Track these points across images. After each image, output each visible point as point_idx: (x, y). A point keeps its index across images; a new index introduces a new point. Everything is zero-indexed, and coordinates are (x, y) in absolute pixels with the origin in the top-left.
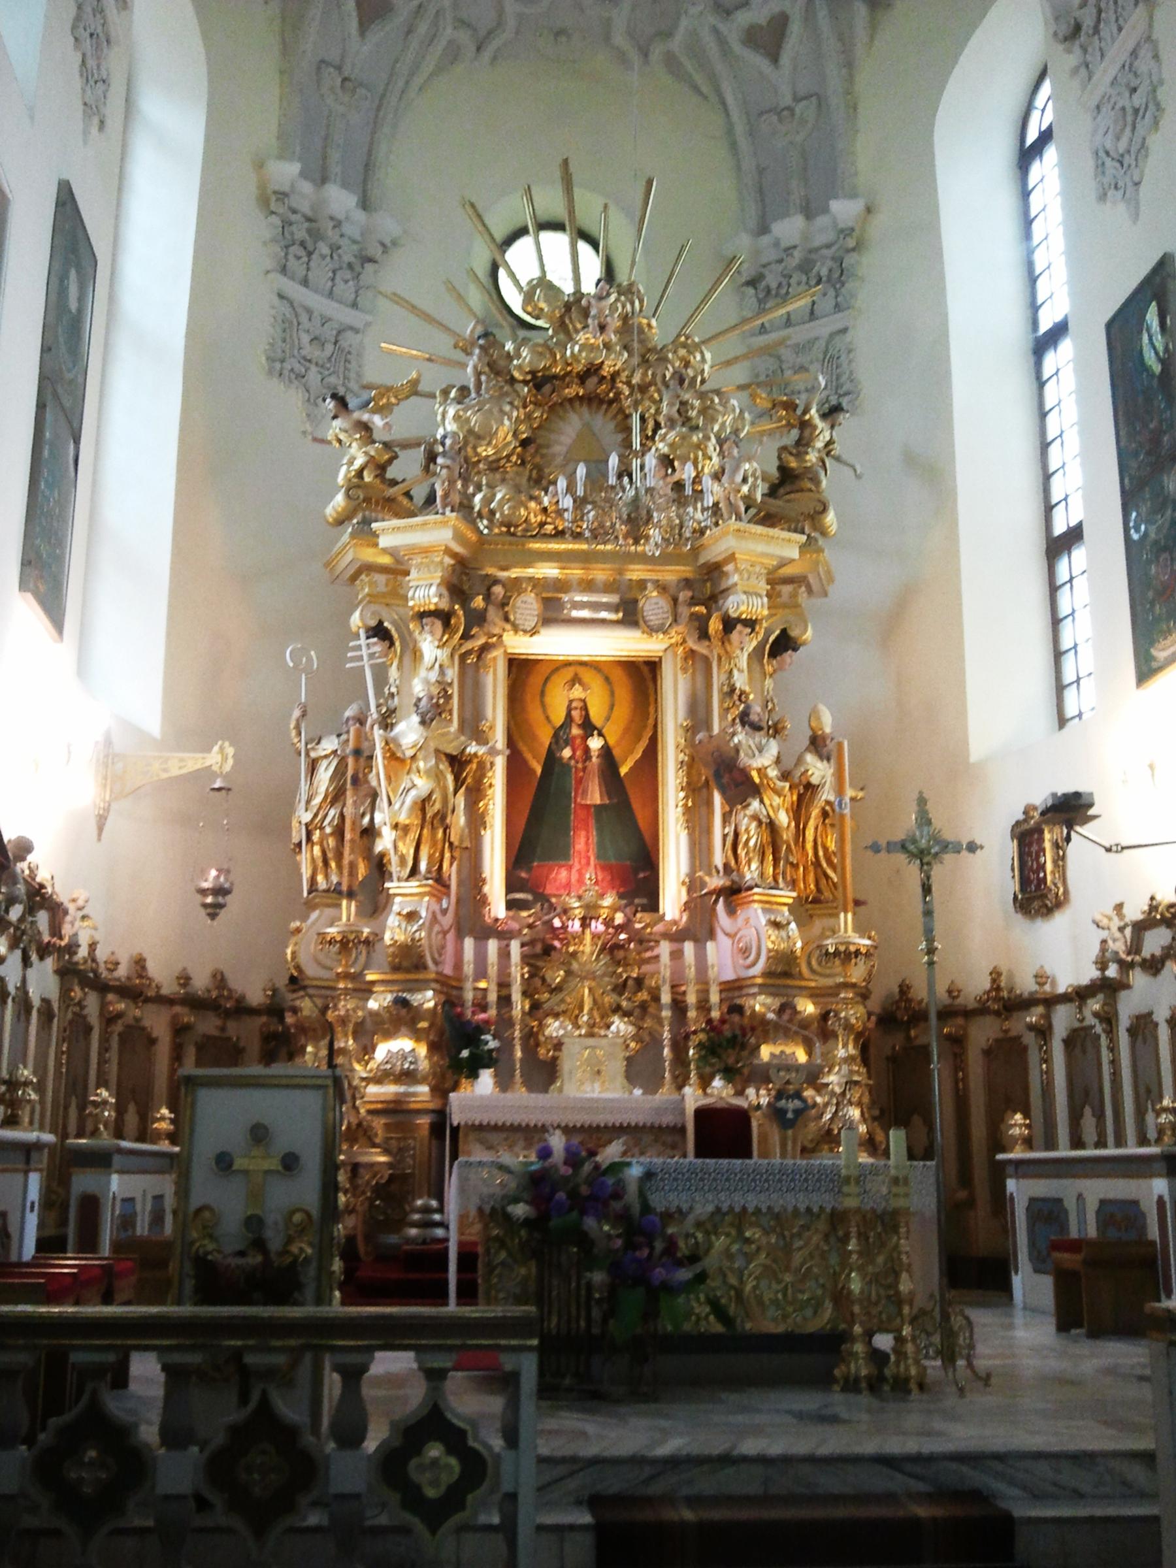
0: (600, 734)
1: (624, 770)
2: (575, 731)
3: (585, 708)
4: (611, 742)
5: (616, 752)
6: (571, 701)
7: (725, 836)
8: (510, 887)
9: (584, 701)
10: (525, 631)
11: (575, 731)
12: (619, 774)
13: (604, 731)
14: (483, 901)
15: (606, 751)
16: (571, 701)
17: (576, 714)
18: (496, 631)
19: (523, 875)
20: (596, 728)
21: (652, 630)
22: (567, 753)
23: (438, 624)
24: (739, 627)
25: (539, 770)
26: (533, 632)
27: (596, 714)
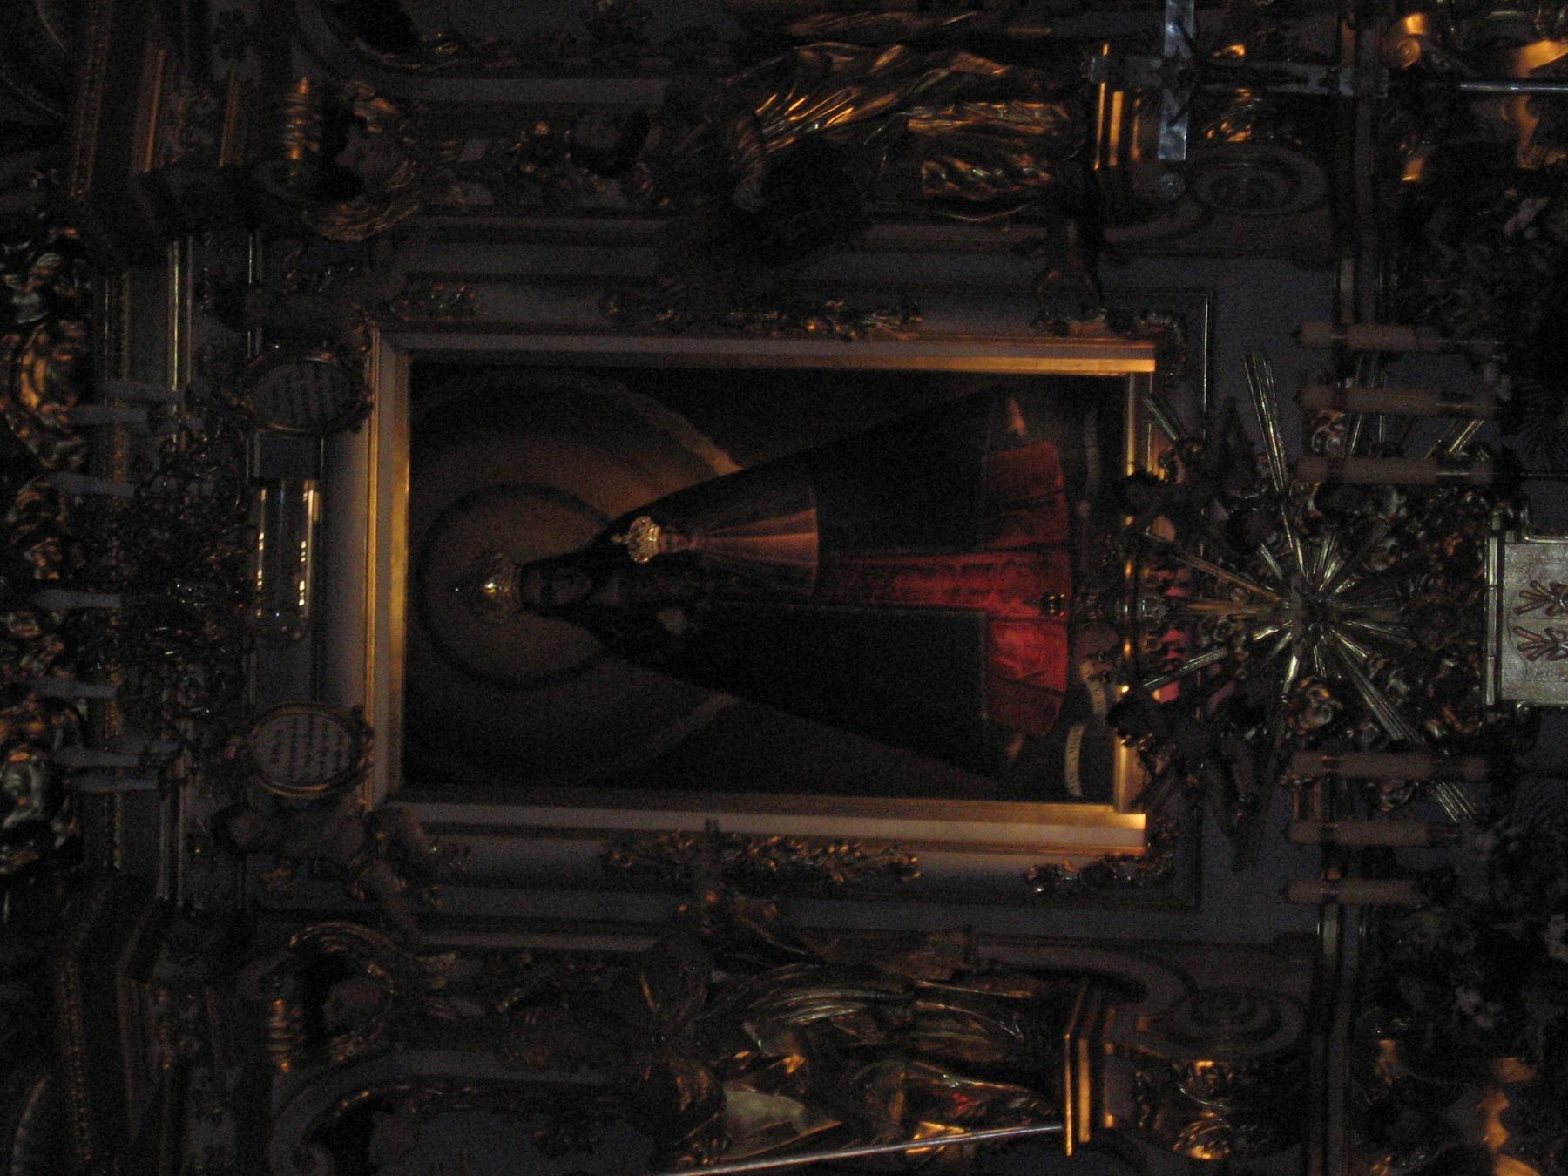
0: (624, 524)
1: (725, 465)
2: (612, 595)
3: (548, 566)
4: (645, 496)
5: (674, 482)
6: (527, 605)
7: (935, 220)
8: (1060, 794)
9: (526, 569)
10: (357, 752)
11: (612, 595)
12: (735, 476)
13: (613, 515)
14: (1103, 874)
15: (665, 511)
16: (527, 605)
17: (564, 593)
18: (356, 833)
19: (1014, 749)
20: (604, 538)
21: (354, 413)
22: (674, 621)
23: (339, 992)
24: (345, 159)
25: (721, 701)
26: (357, 726)
27: (561, 535)
